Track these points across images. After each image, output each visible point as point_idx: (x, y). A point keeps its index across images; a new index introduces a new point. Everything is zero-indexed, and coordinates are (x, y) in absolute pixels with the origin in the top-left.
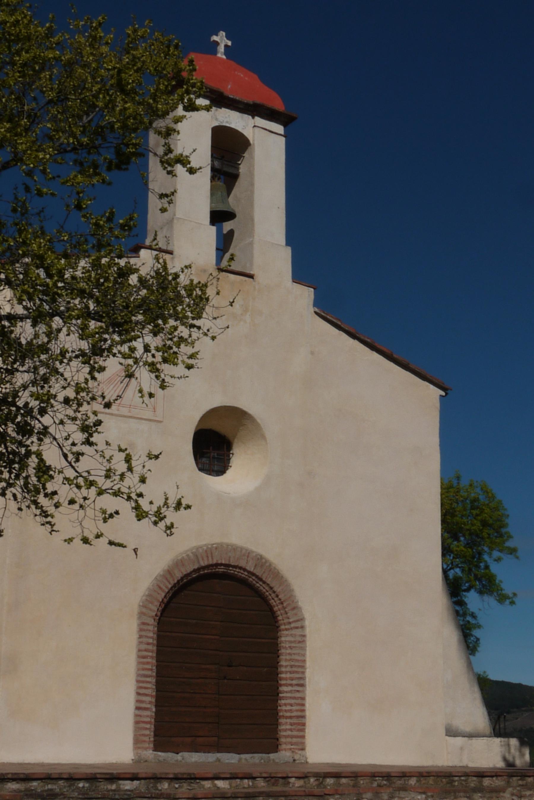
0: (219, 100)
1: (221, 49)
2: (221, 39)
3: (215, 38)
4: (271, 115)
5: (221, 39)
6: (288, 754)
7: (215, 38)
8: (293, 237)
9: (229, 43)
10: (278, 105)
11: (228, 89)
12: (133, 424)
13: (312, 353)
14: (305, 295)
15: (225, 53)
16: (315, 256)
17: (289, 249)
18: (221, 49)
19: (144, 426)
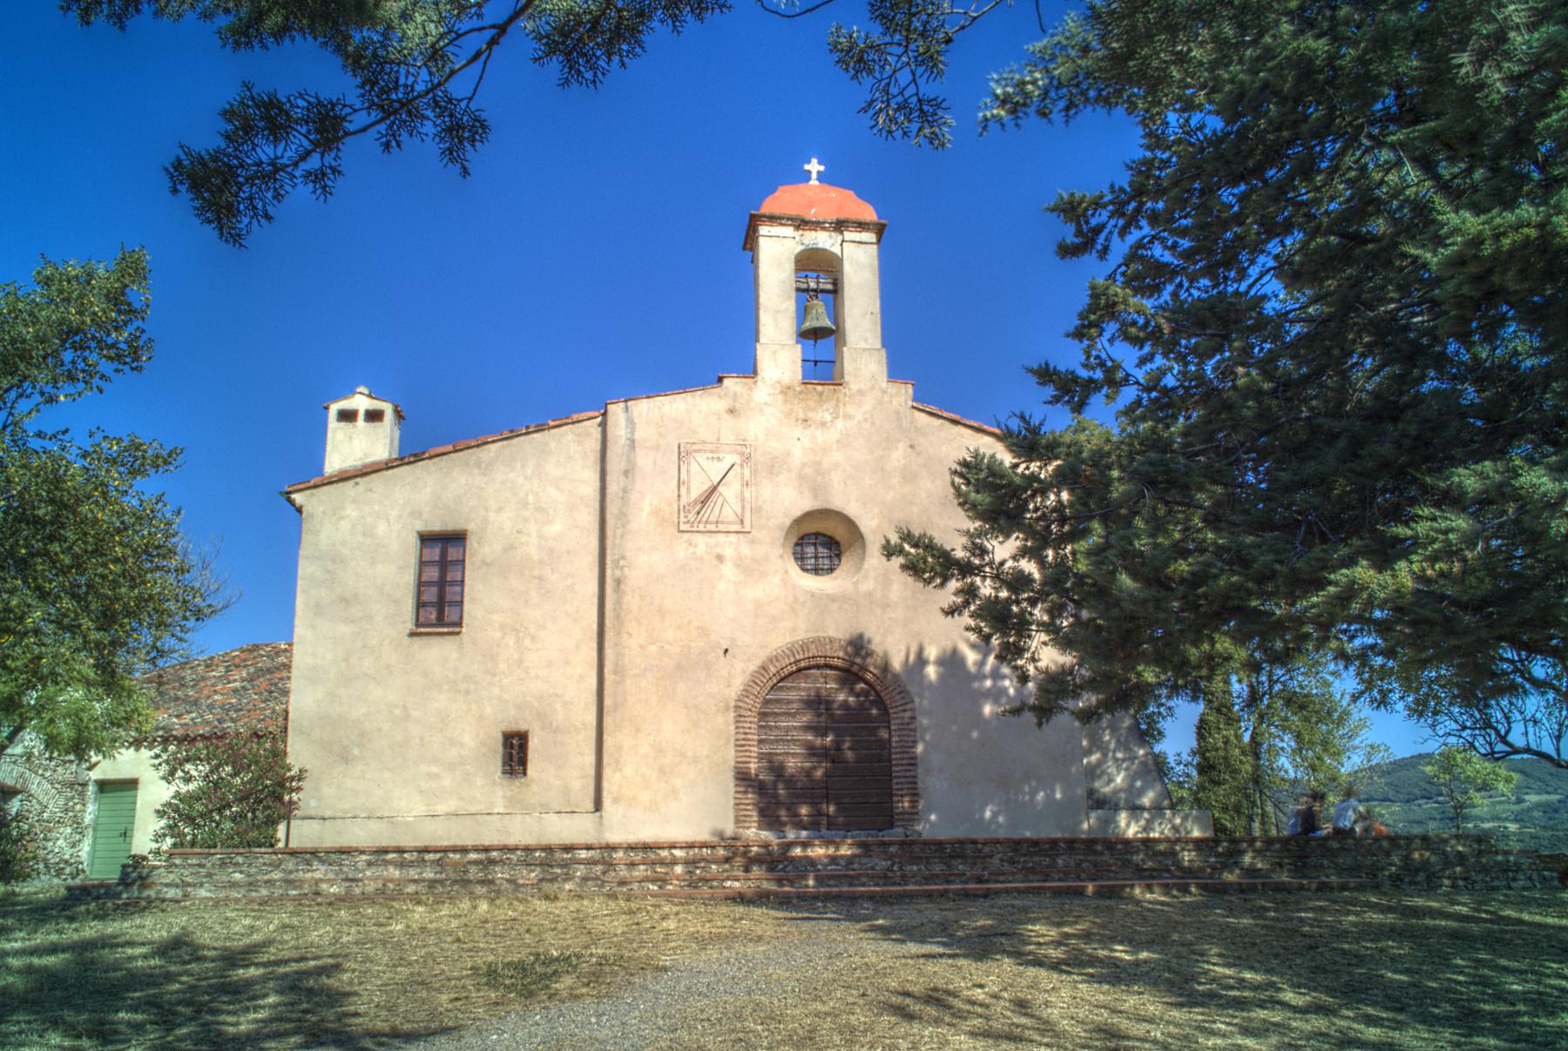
0: (802, 224)
1: (814, 176)
2: (814, 167)
3: (807, 167)
4: (862, 226)
5: (814, 167)
6: (900, 830)
7: (807, 167)
8: (888, 339)
9: (822, 168)
10: (870, 214)
11: (812, 214)
12: (721, 537)
13: (912, 447)
14: (902, 394)
15: (819, 179)
16: (906, 356)
17: (883, 352)
18: (814, 176)
19: (733, 538)
